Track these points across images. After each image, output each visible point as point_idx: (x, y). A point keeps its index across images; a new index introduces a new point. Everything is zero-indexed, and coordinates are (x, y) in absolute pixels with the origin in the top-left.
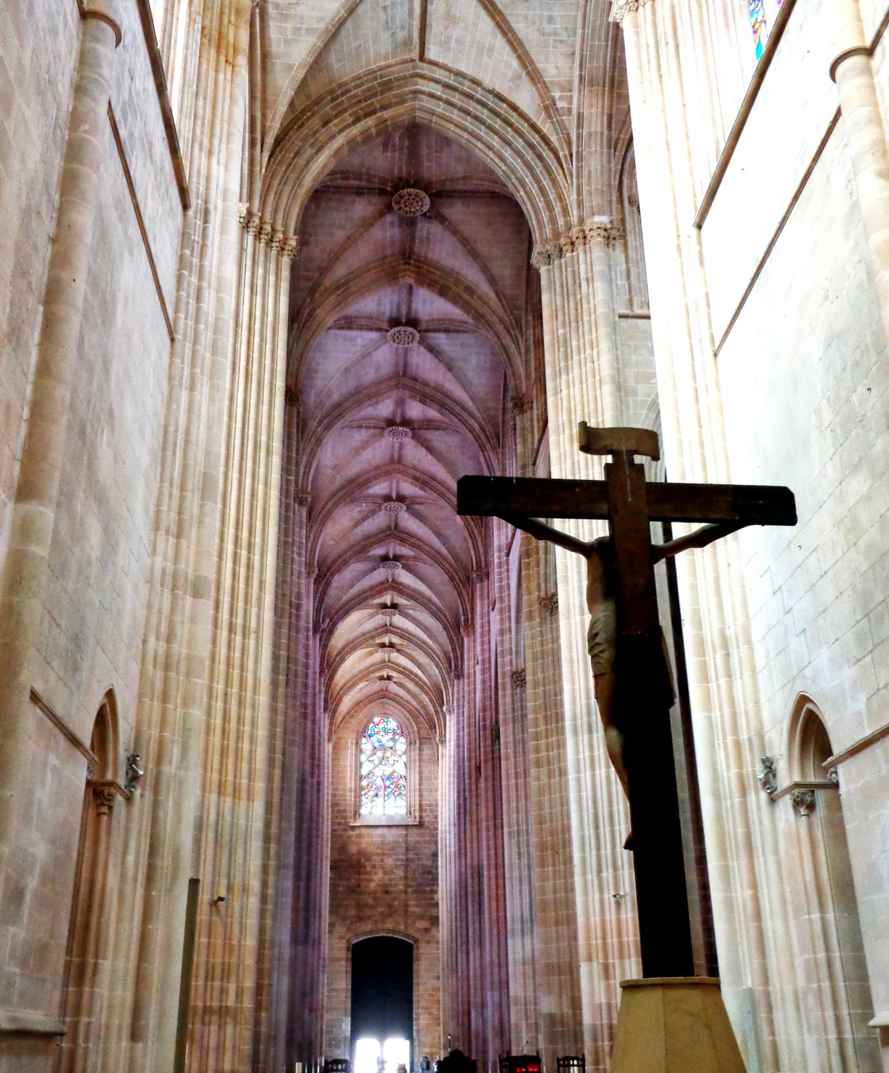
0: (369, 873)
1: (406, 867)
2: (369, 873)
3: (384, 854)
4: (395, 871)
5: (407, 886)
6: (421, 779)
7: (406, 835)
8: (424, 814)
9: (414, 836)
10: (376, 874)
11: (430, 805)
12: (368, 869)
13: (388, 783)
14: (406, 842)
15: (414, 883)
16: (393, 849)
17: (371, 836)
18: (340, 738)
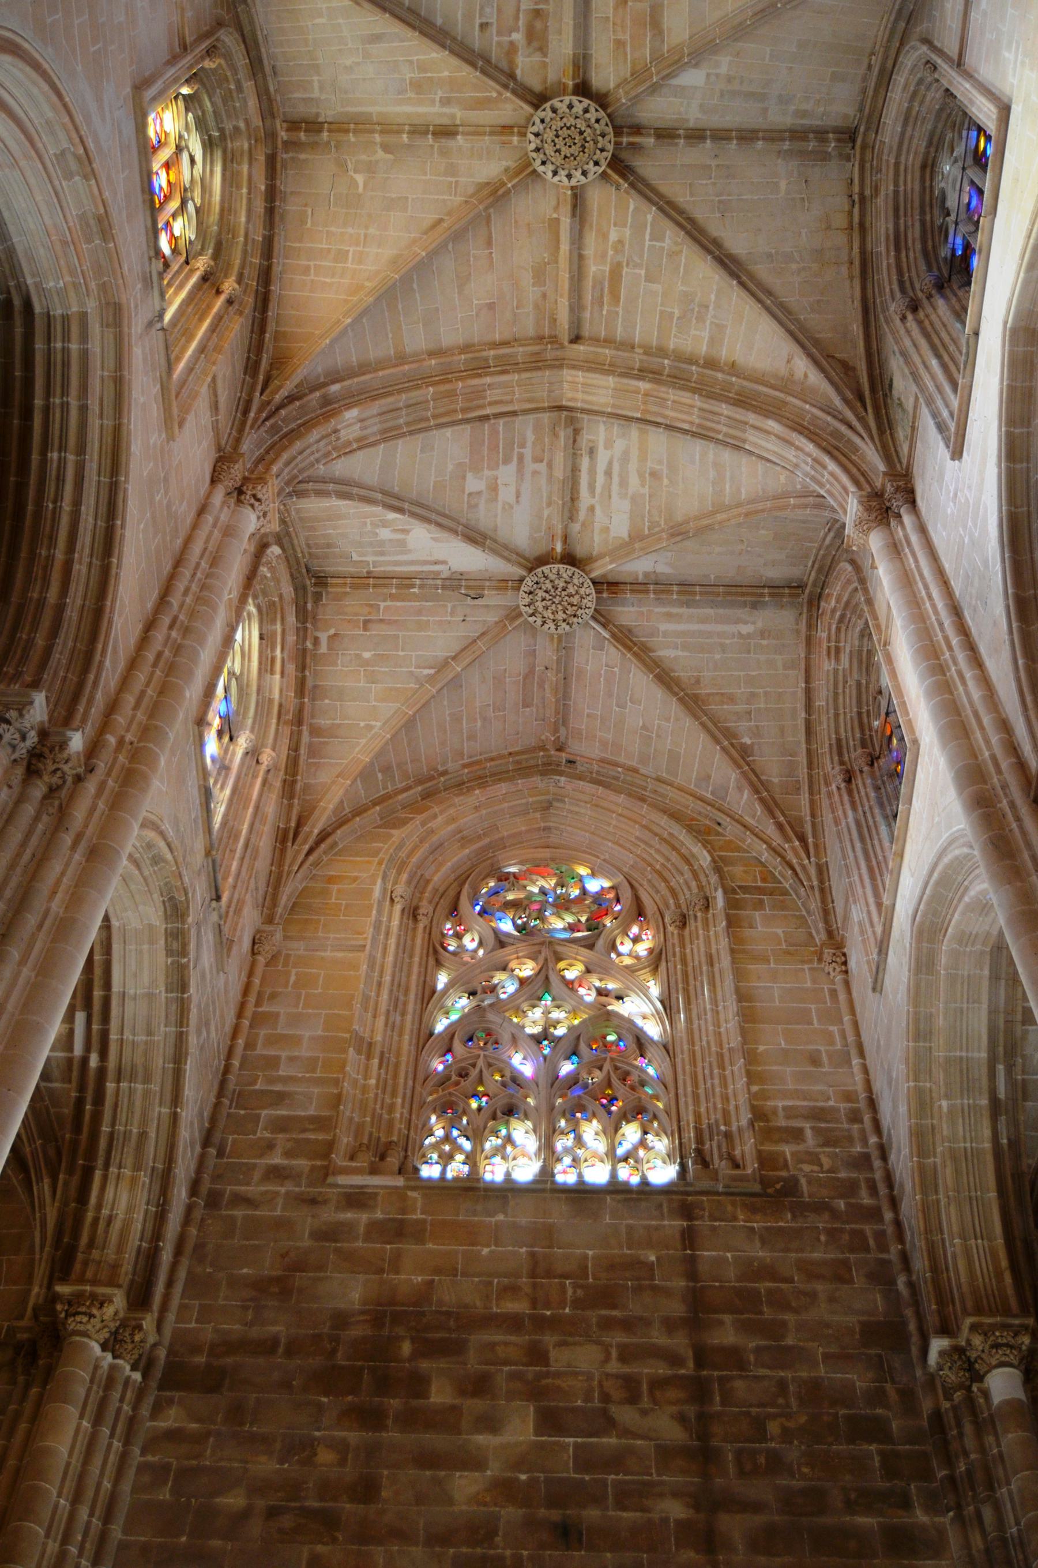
0: (446, 1420)
1: (699, 1390)
2: (446, 1420)
3: (541, 1324)
4: (625, 1415)
5: (709, 1503)
6: (748, 1016)
7: (689, 1238)
8: (787, 1150)
9: (732, 1249)
10: (490, 1424)
11: (817, 1115)
12: (440, 1395)
13: (566, 1068)
14: (691, 1269)
15: (760, 1489)
16: (605, 1296)
17: (471, 1235)
18: (330, 880)
